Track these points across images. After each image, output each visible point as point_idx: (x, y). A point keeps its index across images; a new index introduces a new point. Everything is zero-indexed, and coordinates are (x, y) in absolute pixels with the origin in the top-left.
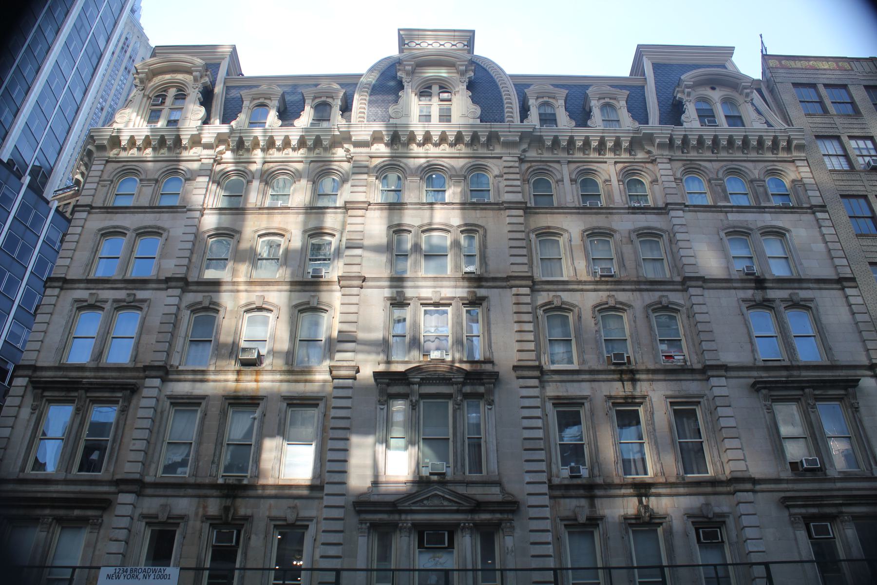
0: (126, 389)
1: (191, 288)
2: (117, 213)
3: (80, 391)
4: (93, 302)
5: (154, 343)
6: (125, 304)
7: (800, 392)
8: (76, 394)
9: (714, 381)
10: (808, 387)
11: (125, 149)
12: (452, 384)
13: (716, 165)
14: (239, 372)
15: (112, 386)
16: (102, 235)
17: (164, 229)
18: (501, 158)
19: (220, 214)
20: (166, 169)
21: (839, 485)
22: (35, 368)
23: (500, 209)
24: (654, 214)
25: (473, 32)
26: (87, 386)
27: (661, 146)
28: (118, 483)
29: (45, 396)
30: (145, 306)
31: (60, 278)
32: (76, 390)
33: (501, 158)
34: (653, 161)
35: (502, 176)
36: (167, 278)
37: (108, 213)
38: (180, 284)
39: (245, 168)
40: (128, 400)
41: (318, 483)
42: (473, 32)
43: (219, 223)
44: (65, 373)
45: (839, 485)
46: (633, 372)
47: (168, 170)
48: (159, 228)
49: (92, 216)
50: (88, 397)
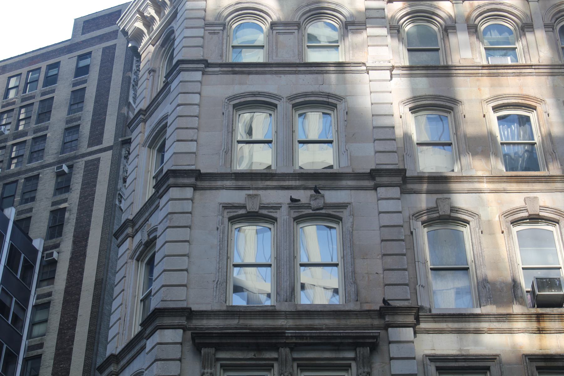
0: (363, 345)
1: (410, 186)
2: (249, 73)
3: (282, 350)
4: (256, 209)
5: (381, 271)
6: (310, 211)
8: (274, 355)
14: (539, 318)
15: (338, 341)
16: (235, 106)
17: (339, 98)
19: (410, 76)
20: (308, 9)
22: (189, 313)
26: (294, 341)
29: (218, 360)
30: (345, 214)
31: (192, 171)
32: (275, 347)
36: (371, 170)
37: (235, 73)
38: (398, 180)
39: (431, 6)
40: (367, 362)
43: (413, 90)
44: (242, 322)
47: (310, 11)
48: (329, 95)
49: (207, 78)
50: (294, 360)
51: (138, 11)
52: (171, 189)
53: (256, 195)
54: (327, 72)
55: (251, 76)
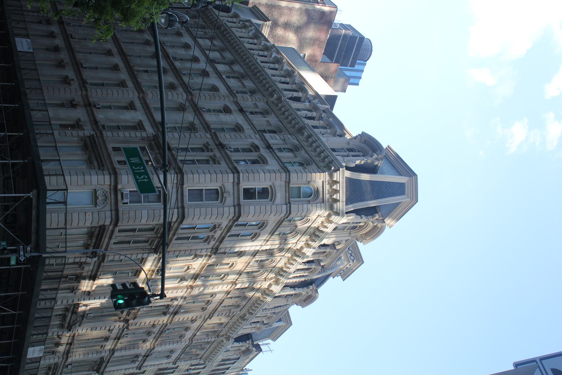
2: (277, 224)
7: (97, 364)
8: (159, 236)
9: (107, 353)
10: (98, 367)
11: (322, 222)
12: (126, 315)
13: (208, 347)
18: (240, 311)
21: (60, 370)
23: (211, 313)
24: (191, 337)
25: (343, 280)
27: (223, 341)
28: (104, 256)
33: (240, 311)
34: (218, 336)
35: (229, 312)
37: (279, 222)
41: (91, 294)
42: (343, 280)
45: (60, 370)
46: (119, 339)
51: (339, 182)
52: (234, 215)
53: (221, 230)
54: (267, 237)
55: (275, 224)
